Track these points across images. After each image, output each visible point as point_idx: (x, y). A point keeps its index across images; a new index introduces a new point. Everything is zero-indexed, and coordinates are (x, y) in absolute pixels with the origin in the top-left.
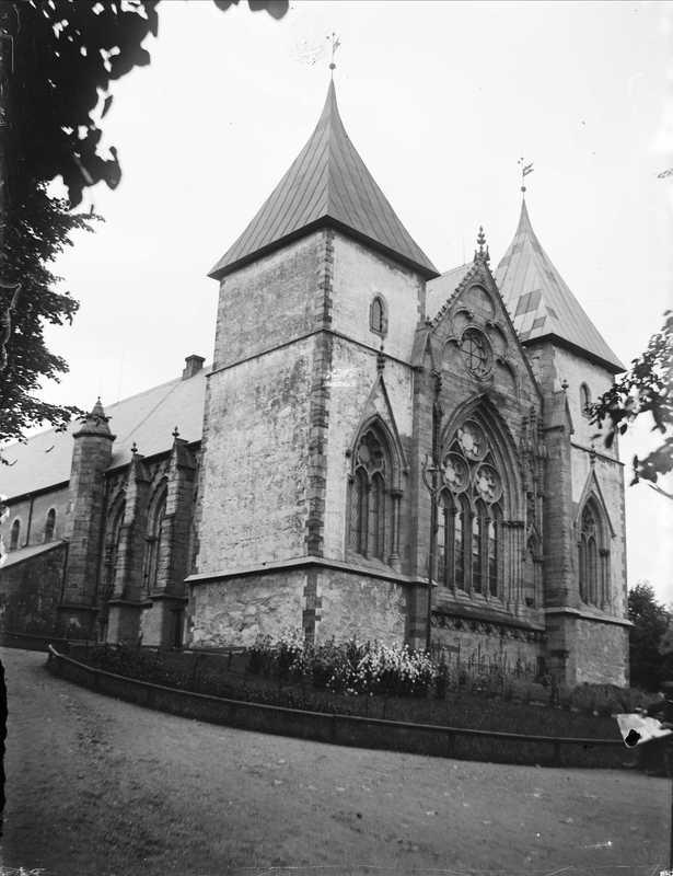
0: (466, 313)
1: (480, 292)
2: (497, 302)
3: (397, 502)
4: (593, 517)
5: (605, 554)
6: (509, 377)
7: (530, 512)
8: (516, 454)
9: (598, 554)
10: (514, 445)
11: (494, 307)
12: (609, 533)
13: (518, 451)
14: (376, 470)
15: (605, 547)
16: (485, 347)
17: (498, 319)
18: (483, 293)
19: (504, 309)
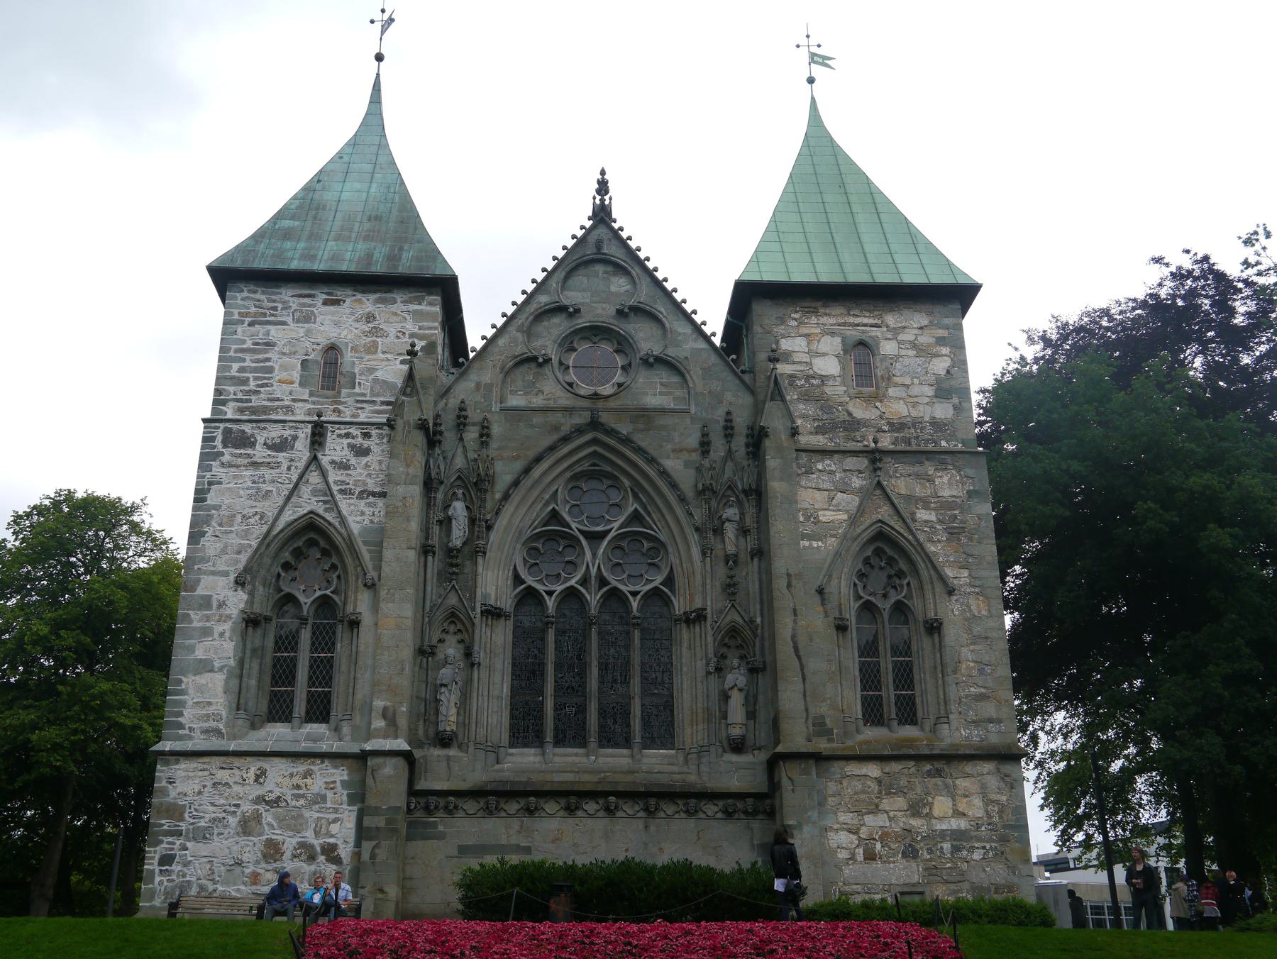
0: (560, 309)
1: (600, 268)
2: (635, 271)
3: (355, 630)
4: (903, 565)
5: (934, 628)
6: (675, 379)
7: (730, 589)
8: (682, 499)
9: (922, 629)
10: (674, 486)
11: (633, 282)
12: (939, 589)
13: (690, 494)
14: (318, 593)
15: (931, 615)
16: (623, 345)
17: (644, 294)
18: (610, 268)
19: (650, 273)
